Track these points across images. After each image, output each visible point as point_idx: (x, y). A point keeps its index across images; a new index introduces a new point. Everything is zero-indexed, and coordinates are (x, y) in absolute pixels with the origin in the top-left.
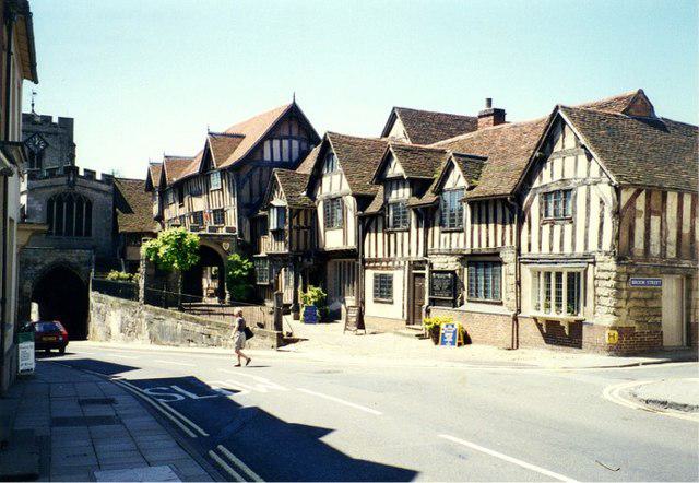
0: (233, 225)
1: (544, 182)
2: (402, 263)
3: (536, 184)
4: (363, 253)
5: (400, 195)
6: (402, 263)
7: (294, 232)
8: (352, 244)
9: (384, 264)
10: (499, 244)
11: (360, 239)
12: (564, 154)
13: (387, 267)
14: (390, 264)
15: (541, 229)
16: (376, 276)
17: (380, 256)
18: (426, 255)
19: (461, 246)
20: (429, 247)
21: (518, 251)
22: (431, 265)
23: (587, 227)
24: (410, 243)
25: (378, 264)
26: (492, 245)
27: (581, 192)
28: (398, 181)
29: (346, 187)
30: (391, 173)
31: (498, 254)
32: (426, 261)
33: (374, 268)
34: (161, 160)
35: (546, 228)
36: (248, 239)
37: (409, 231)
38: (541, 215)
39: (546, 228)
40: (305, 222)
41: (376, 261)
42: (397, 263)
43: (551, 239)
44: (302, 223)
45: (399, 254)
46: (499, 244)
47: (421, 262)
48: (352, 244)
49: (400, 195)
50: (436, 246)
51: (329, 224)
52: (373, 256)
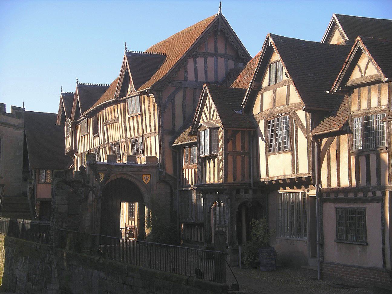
0: (154, 155)
4: (320, 181)
5: (374, 103)
7: (230, 158)
8: (304, 169)
13: (356, 200)
29: (295, 98)
30: (356, 75)
34: (72, 89)
36: (169, 169)
40: (243, 147)
42: (370, 194)
44: (239, 148)
48: (304, 169)
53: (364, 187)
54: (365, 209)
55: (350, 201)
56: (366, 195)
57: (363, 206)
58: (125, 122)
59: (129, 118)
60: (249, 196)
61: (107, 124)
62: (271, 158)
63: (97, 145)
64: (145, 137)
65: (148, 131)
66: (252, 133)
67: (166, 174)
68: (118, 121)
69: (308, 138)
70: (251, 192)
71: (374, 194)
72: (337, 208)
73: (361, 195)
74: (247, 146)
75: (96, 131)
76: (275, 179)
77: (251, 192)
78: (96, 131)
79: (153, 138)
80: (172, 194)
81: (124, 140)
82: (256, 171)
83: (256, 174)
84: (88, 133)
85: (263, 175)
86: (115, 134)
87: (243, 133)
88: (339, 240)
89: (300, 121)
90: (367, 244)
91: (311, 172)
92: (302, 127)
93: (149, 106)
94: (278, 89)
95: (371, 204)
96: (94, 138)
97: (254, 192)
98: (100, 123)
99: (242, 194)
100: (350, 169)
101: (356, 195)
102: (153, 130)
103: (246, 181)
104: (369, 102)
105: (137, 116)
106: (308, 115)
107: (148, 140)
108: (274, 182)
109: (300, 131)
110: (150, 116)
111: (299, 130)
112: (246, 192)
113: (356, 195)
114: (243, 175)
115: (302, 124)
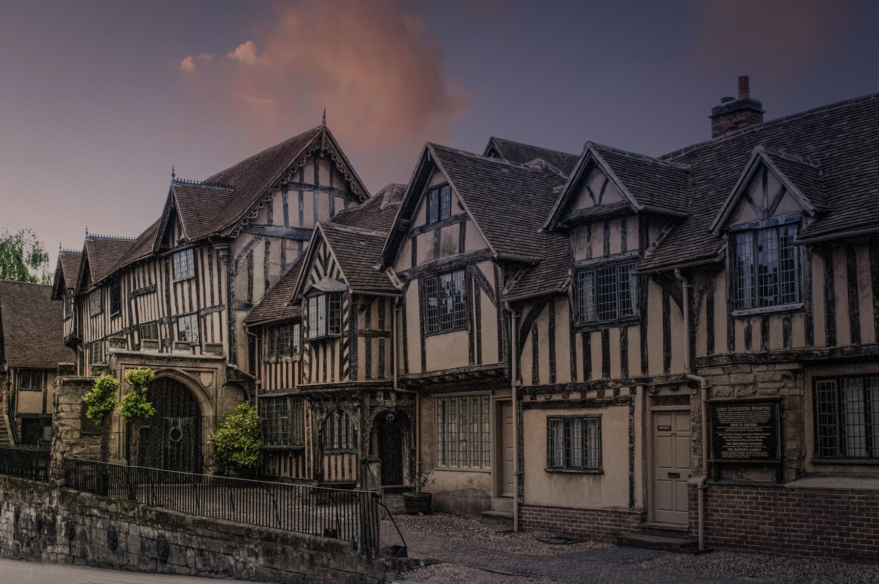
4: (518, 376)
5: (615, 248)
8: (490, 357)
9: (575, 396)
13: (584, 404)
14: (592, 395)
16: (552, 422)
17: (564, 376)
18: (694, 364)
19: (798, 341)
20: (702, 351)
25: (557, 397)
32: (694, 384)
33: (549, 405)
37: (642, 322)
42: (609, 393)
45: (616, 373)
47: (676, 386)
48: (490, 357)
49: (615, 248)
50: (721, 347)
52: (544, 379)
53: (599, 382)
54: (599, 418)
55: (572, 405)
56: (601, 395)
57: (594, 412)
69: (498, 305)
71: (617, 392)
72: (548, 418)
73: (592, 395)
74: (387, 322)
76: (439, 373)
82: (402, 362)
83: (402, 367)
85: (415, 368)
89: (485, 279)
91: (505, 358)
92: (488, 291)
95: (611, 409)
97: (399, 396)
100: (573, 354)
101: (584, 395)
104: (607, 247)
106: (499, 269)
108: (435, 380)
109: (484, 296)
111: (482, 292)
113: (584, 395)
115: (488, 284)
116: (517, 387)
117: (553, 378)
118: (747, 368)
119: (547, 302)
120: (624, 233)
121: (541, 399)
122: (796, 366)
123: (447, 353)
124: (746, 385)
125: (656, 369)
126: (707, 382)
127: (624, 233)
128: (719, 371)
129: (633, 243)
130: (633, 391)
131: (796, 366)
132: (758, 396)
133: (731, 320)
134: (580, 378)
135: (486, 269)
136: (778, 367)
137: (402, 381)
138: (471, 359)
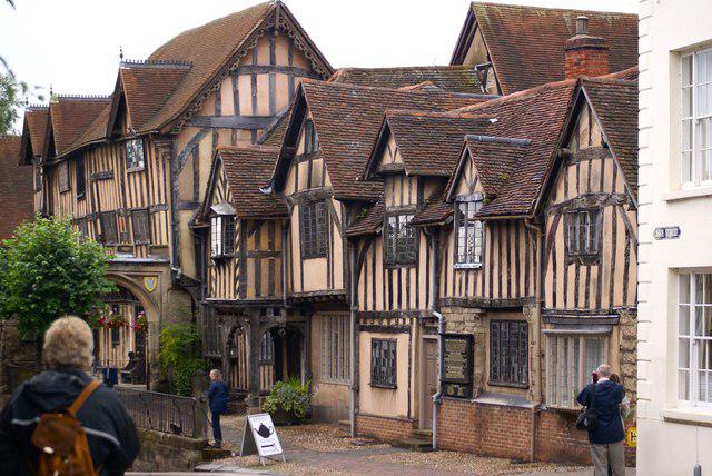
0: (164, 243)
1: (570, 197)
2: (408, 321)
3: (561, 198)
6: (408, 321)
8: (339, 285)
9: (385, 323)
10: (522, 294)
11: (352, 275)
12: (587, 155)
13: (389, 330)
14: (393, 322)
15: (566, 270)
16: (375, 343)
17: (380, 307)
20: (442, 295)
21: (543, 304)
22: (444, 324)
23: (613, 270)
24: (416, 287)
26: (513, 295)
27: (608, 210)
28: (398, 174)
30: (387, 160)
31: (520, 310)
32: (436, 319)
33: (372, 329)
35: (572, 268)
36: (188, 268)
37: (416, 264)
38: (566, 249)
39: (572, 268)
40: (271, 245)
41: (375, 315)
43: (577, 279)
46: (522, 294)
50: (450, 293)
51: (308, 254)
54: (395, 342)
57: (394, 337)
58: (123, 180)
59: (129, 174)
60: (282, 318)
61: (98, 178)
62: (307, 262)
63: (83, 213)
64: (152, 210)
65: (157, 202)
66: (284, 223)
67: (182, 275)
68: (112, 178)
69: (343, 238)
70: (283, 312)
75: (81, 188)
76: (310, 295)
77: (283, 312)
78: (81, 188)
79: (163, 213)
80: (194, 308)
81: (122, 211)
83: (290, 286)
84: (70, 189)
85: (298, 288)
86: (109, 197)
87: (272, 223)
88: (373, 385)
90: (396, 388)
92: (338, 224)
93: (157, 158)
94: (314, 161)
96: (79, 199)
97: (290, 313)
98: (87, 176)
99: (270, 315)
100: (384, 287)
101: (389, 323)
102: (163, 202)
103: (277, 295)
105: (140, 172)
107: (157, 215)
110: (158, 177)
112: (277, 313)
113: (389, 323)
114: (272, 286)
116: (356, 312)
117: (374, 305)
118: (460, 309)
119: (372, 238)
120: (410, 188)
121: (369, 323)
122: (479, 311)
123: (314, 277)
124: (460, 323)
125: (422, 306)
126: (444, 318)
127: (410, 188)
128: (448, 310)
129: (414, 200)
130: (412, 323)
131: (479, 311)
132: (466, 332)
133: (455, 270)
134: (387, 309)
135: (337, 205)
136: (473, 310)
137: (290, 299)
138: (329, 285)
